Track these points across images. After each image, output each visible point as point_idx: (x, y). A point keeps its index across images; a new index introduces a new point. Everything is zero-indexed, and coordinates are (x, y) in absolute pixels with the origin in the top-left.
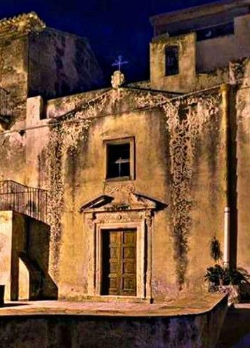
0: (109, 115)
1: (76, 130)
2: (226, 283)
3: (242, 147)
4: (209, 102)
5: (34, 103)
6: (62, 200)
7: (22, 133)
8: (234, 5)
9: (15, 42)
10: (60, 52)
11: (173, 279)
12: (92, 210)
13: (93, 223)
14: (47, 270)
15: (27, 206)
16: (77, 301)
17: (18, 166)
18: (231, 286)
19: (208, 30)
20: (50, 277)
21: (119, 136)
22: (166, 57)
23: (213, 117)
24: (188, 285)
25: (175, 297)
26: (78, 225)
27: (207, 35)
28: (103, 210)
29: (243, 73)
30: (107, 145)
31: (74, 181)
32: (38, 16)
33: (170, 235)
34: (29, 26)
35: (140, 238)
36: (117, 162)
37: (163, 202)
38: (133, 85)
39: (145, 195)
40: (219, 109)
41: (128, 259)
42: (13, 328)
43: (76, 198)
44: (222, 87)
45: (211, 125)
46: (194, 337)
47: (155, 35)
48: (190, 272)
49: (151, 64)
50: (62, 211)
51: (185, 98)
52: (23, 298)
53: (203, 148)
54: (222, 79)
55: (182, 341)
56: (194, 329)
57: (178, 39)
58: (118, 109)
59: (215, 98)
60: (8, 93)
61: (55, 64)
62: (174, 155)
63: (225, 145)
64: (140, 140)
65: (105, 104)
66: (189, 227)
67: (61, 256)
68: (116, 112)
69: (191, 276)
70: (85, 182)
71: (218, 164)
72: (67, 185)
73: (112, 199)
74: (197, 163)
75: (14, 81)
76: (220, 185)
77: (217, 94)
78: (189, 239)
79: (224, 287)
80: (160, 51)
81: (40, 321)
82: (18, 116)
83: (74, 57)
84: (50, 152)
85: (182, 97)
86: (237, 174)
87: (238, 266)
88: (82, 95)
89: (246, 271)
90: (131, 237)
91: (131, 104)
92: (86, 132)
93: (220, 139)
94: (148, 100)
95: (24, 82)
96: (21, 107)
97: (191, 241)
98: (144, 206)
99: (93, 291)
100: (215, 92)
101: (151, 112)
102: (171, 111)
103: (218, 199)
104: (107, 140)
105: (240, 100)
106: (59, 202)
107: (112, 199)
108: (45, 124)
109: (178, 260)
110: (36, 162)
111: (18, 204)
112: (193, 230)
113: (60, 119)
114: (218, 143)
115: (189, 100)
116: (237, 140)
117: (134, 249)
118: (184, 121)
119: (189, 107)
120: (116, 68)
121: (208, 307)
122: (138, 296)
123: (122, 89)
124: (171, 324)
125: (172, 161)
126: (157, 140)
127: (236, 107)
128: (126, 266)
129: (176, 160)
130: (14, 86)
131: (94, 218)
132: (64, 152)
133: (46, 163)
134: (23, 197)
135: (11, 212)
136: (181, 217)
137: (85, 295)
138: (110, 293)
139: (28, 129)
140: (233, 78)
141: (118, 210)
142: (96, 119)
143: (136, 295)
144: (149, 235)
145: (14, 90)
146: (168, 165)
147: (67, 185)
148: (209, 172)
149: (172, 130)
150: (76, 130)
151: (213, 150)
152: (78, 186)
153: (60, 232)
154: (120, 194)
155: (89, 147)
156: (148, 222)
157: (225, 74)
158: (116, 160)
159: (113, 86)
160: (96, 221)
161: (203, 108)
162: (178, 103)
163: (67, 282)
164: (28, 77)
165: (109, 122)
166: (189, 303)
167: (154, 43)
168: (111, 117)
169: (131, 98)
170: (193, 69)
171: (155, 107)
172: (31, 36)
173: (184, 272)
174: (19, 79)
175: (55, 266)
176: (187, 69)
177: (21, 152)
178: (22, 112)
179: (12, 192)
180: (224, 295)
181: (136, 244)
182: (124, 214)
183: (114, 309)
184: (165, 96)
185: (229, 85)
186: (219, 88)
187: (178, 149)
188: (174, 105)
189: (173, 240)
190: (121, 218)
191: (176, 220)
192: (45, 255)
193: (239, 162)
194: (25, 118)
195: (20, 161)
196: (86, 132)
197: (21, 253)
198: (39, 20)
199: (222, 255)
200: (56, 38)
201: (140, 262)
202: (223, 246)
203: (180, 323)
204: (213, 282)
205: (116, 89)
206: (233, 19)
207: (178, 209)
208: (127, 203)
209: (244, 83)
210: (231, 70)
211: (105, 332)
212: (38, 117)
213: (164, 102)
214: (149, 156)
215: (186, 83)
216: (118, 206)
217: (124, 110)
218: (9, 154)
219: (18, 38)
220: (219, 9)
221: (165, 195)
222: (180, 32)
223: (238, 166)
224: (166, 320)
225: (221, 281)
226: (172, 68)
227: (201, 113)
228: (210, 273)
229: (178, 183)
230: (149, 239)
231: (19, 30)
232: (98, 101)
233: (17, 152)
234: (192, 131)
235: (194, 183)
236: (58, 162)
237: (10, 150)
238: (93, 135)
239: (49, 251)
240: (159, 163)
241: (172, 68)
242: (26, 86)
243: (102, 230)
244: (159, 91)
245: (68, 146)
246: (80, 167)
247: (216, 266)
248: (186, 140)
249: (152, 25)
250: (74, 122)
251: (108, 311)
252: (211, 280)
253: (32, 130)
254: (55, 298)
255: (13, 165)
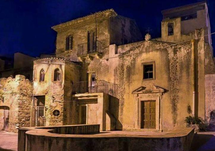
0: (144, 52)
1: (130, 59)
2: (194, 123)
3: (200, 66)
4: (186, 47)
5: (112, 47)
6: (124, 88)
7: (107, 60)
8: (197, 6)
9: (104, 21)
10: (124, 26)
11: (171, 122)
12: (137, 93)
13: (137, 98)
14: (118, 118)
15: (110, 91)
16: (131, 131)
17: (106, 74)
18: (196, 125)
19: (186, 16)
20: (119, 121)
21: (148, 61)
22: (168, 28)
23: (188, 53)
24: (177, 124)
25: (172, 130)
26: (131, 99)
27: (186, 19)
28: (142, 93)
29: (201, 34)
30: (143, 65)
31: (129, 80)
32: (114, 10)
33: (170, 103)
34: (110, 14)
35: (157, 104)
36: (147, 72)
37: (167, 89)
38: (154, 39)
39: (159, 86)
40: (191, 50)
41: (152, 114)
42: (103, 143)
43: (130, 87)
44: (192, 40)
45: (187, 57)
46: (180, 146)
47: (163, 18)
48: (178, 119)
49: (162, 31)
50: (124, 93)
51: (176, 45)
52: (108, 130)
53: (184, 66)
54: (192, 37)
55: (175, 148)
56: (180, 143)
57: (173, 20)
58: (148, 50)
59: (189, 45)
60: (101, 43)
61: (121, 31)
62: (172, 69)
63: (193, 65)
64: (157, 63)
65: (142, 48)
66: (178, 100)
67: (124, 112)
68: (147, 51)
69: (179, 121)
70: (134, 81)
71: (190, 73)
72: (126, 82)
73: (145, 88)
74: (181, 73)
75: (104, 38)
76: (191, 82)
77: (190, 43)
78: (178, 105)
79: (193, 125)
80: (165, 25)
81: (115, 139)
82: (105, 53)
83: (129, 28)
84: (119, 68)
85: (175, 44)
86: (198, 77)
87: (199, 116)
88: (133, 44)
89: (202, 118)
90: (154, 104)
91: (153, 48)
92: (134, 59)
93: (191, 62)
94: (161, 46)
95: (108, 38)
96: (107, 49)
97: (179, 106)
98: (159, 91)
99: (137, 127)
100: (189, 43)
101: (162, 51)
102: (170, 51)
103: (190, 88)
104: (143, 63)
105: (199, 46)
106: (123, 89)
107: (145, 88)
108: (117, 56)
109: (173, 113)
110: (113, 72)
111: (106, 90)
112: (180, 101)
113: (123, 54)
114: (190, 64)
115: (178, 46)
116: (198, 63)
117: (154, 109)
118: (176, 55)
119: (178, 49)
120: (147, 33)
121: (186, 134)
122: (156, 129)
123: (149, 41)
124: (170, 141)
125: (171, 72)
126: (164, 63)
127: (198, 49)
128: (151, 116)
129: (173, 71)
130: (104, 40)
131: (138, 96)
132: (125, 68)
133: (118, 73)
134: (108, 87)
135: (103, 93)
136: (174, 96)
137: (134, 129)
138: (145, 127)
139: (110, 58)
140: (197, 37)
141: (148, 93)
142: (138, 54)
143: (155, 129)
144: (161, 103)
145: (104, 42)
146: (169, 73)
147: (126, 82)
148: (186, 76)
149: (170, 59)
150: (130, 59)
151: (188, 67)
152: (131, 82)
153: (123, 102)
154: (149, 86)
155: (136, 66)
156: (161, 98)
157: (193, 35)
158: (147, 72)
159: (146, 40)
160: (139, 97)
161: (184, 49)
162: (173, 47)
163: (126, 123)
164: (110, 36)
165: (144, 56)
166: (178, 132)
167: (163, 22)
168: (145, 53)
169: (153, 45)
170: (180, 33)
171: (164, 49)
172: (111, 19)
173: (176, 119)
174: (106, 37)
175: (121, 116)
176: (177, 33)
177: (107, 68)
178: (107, 51)
179: (103, 85)
180: (193, 129)
181: (155, 107)
182: (150, 94)
183: (146, 135)
184: (168, 44)
185: (195, 39)
186: (191, 41)
187: (173, 67)
188: (172, 48)
189: (171, 105)
190: (149, 96)
191: (172, 97)
192: (117, 111)
193: (199, 72)
194: (109, 54)
195: (106, 72)
196: (134, 59)
197: (107, 111)
198: (115, 12)
199: (192, 111)
200: (122, 20)
201: (157, 114)
202: (192, 108)
203: (174, 141)
204: (188, 123)
205: (147, 41)
206: (196, 12)
207: (173, 92)
208: (152, 89)
209: (201, 39)
210: (196, 33)
211: (142, 144)
212: (114, 53)
213: (167, 47)
214: (161, 70)
215: (177, 39)
216: (148, 91)
217: (150, 50)
218: (102, 69)
219: (106, 20)
220: (191, 7)
221: (168, 86)
222: (174, 17)
223: (199, 74)
224: (168, 139)
225: (191, 123)
226: (171, 32)
227: (183, 52)
228: (187, 119)
229: (173, 81)
230: (161, 105)
231: (106, 16)
232: (139, 46)
233: (105, 68)
234: (179, 59)
235: (180, 81)
236: (122, 72)
237: (102, 67)
238: (137, 61)
239: (118, 110)
240: (165, 73)
241: (171, 32)
242: (109, 40)
243: (141, 101)
244: (165, 42)
245: (127, 66)
246: (132, 74)
247: (189, 116)
248: (177, 63)
249: (162, 14)
250: (129, 55)
251: (144, 136)
252: (187, 122)
253: (112, 59)
254: (121, 130)
255: (104, 73)
